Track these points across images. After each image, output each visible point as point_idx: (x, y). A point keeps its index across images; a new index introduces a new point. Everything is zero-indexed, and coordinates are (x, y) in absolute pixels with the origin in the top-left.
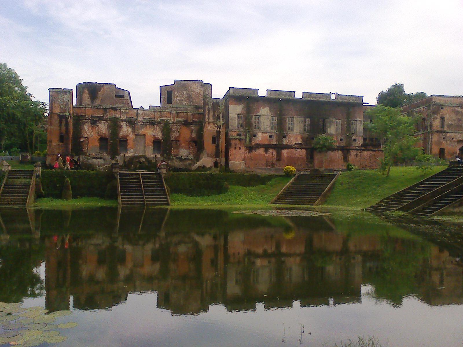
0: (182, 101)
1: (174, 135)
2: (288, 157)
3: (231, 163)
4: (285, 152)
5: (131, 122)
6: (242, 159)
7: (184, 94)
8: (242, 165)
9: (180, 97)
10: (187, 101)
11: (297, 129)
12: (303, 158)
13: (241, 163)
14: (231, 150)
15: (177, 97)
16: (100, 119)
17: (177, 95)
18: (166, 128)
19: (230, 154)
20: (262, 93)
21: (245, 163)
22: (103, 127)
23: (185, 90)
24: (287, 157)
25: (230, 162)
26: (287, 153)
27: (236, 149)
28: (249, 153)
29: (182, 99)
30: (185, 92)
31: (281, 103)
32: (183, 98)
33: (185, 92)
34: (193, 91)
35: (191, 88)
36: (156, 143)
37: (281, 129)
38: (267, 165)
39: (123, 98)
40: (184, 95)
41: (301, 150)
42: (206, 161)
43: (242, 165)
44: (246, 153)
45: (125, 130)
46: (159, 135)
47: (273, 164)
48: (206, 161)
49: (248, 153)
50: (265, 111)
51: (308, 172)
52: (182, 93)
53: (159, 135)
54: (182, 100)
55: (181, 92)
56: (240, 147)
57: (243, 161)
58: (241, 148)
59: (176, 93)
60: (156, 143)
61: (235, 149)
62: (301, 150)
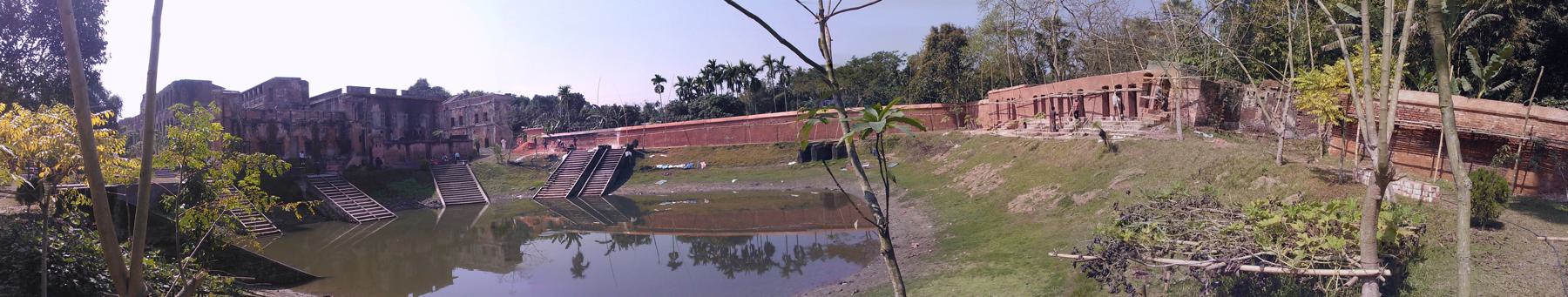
1: (321, 136)
5: (286, 125)
11: (400, 121)
16: (260, 121)
18: (315, 131)
20: (373, 92)
22: (262, 130)
31: (386, 97)
36: (308, 144)
37: (388, 121)
42: (356, 160)
45: (282, 132)
46: (310, 136)
48: (356, 160)
50: (376, 108)
53: (310, 136)
60: (308, 144)
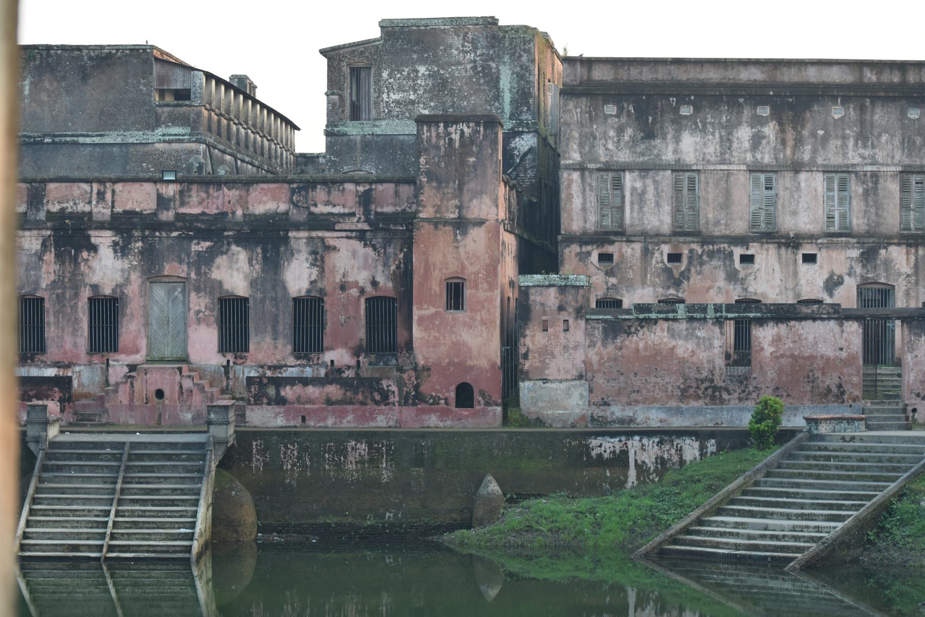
0: (410, 107)
2: (782, 356)
3: (529, 390)
4: (765, 336)
6: (575, 373)
7: (420, 75)
8: (576, 394)
9: (401, 89)
10: (432, 104)
12: (852, 358)
13: (569, 389)
14: (527, 332)
15: (390, 89)
17: (391, 80)
19: (522, 350)
21: (591, 391)
23: (424, 62)
24: (776, 357)
25: (525, 387)
26: (777, 340)
27: (550, 330)
28: (604, 344)
29: (412, 97)
30: (422, 70)
32: (415, 91)
33: (422, 70)
34: (459, 63)
35: (445, 50)
38: (684, 394)
39: (187, 103)
40: (419, 82)
41: (841, 325)
43: (576, 394)
44: (592, 345)
47: (719, 389)
49: (599, 344)
51: (856, 423)
52: (409, 74)
54: (413, 102)
55: (407, 70)
56: (566, 321)
57: (580, 377)
58: (571, 322)
59: (385, 75)
61: (545, 330)
62: (841, 325)
